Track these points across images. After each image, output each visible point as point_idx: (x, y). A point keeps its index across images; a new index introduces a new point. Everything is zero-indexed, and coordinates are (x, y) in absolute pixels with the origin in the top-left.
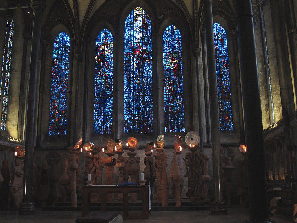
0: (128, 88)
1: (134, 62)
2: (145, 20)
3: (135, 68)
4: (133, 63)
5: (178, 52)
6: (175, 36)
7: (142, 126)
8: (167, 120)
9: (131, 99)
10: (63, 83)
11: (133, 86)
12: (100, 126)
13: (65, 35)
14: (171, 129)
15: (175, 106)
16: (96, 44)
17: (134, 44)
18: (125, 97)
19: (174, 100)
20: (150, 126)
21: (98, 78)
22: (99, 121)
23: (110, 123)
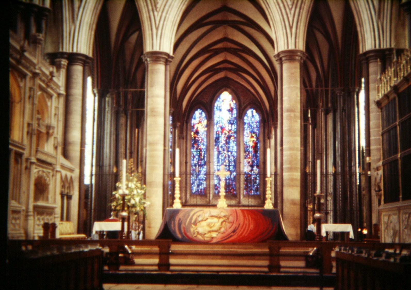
8: (247, 185)
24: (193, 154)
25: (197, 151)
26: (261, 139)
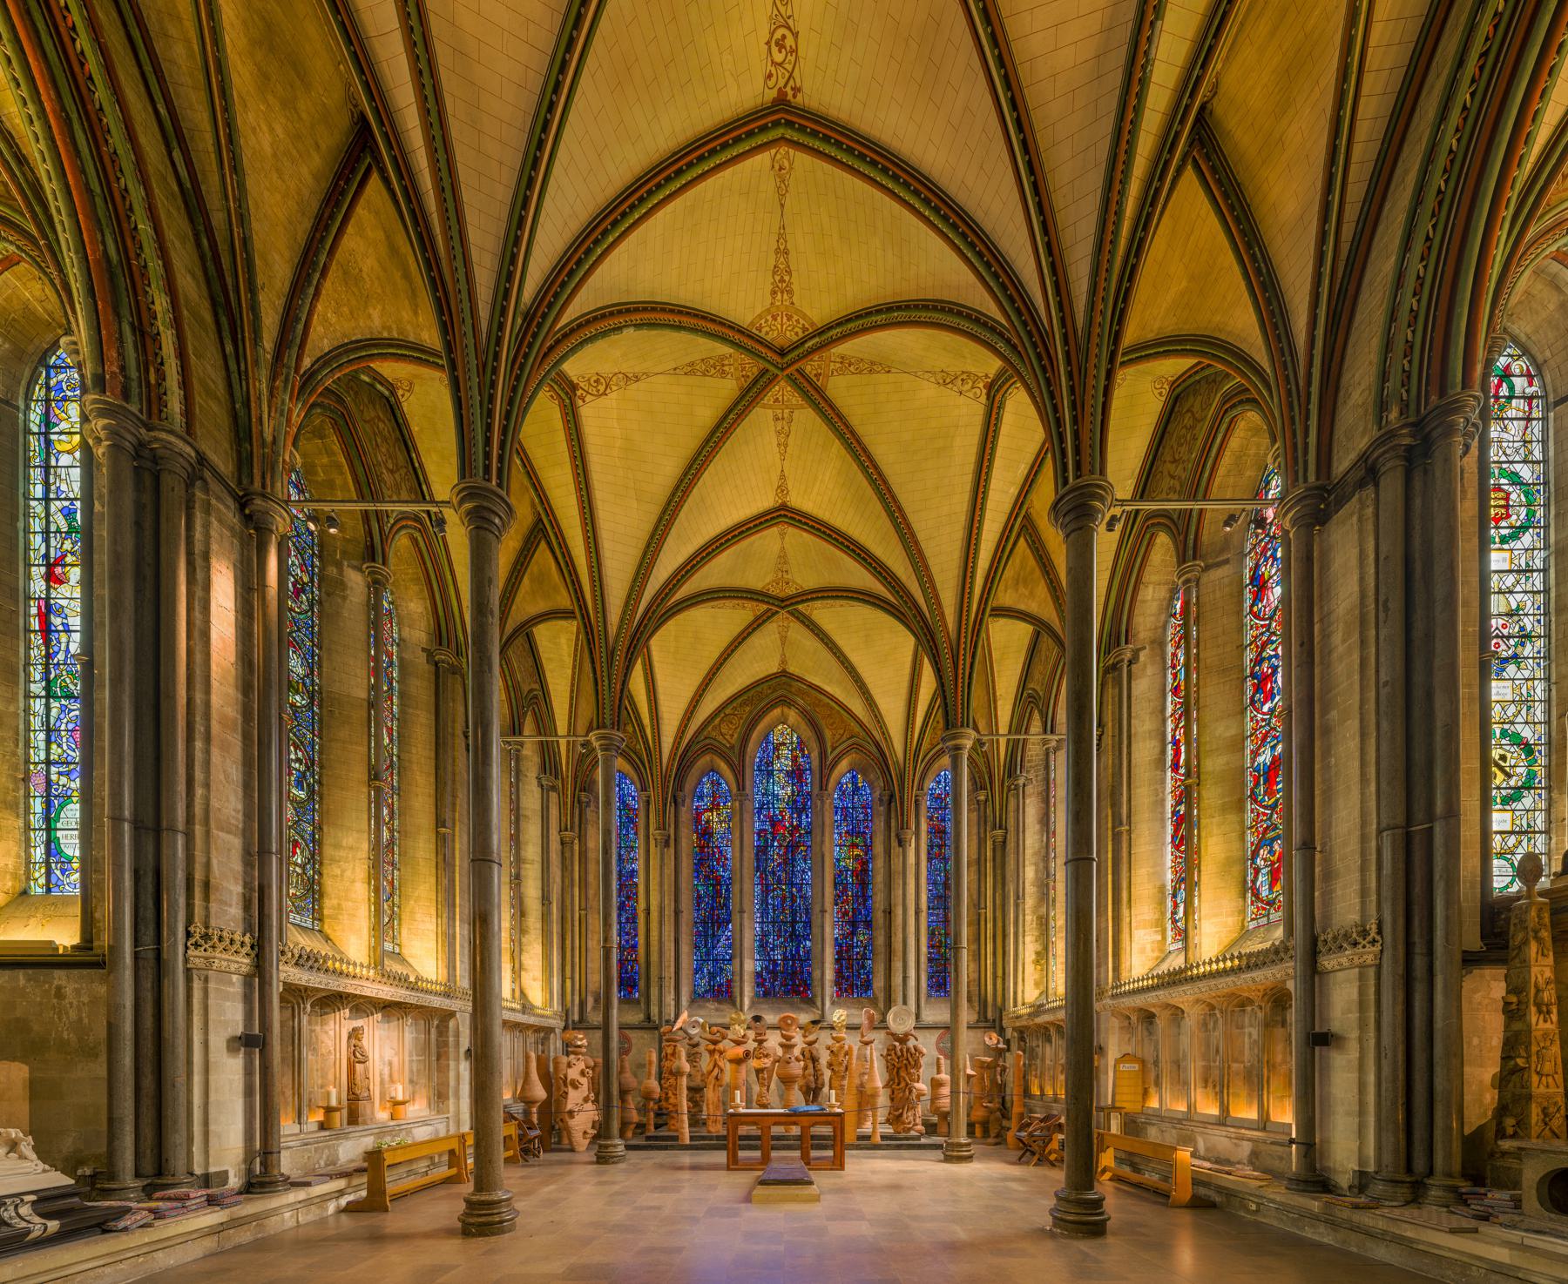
14: (846, 991)
19: (853, 933)
25: (707, 886)
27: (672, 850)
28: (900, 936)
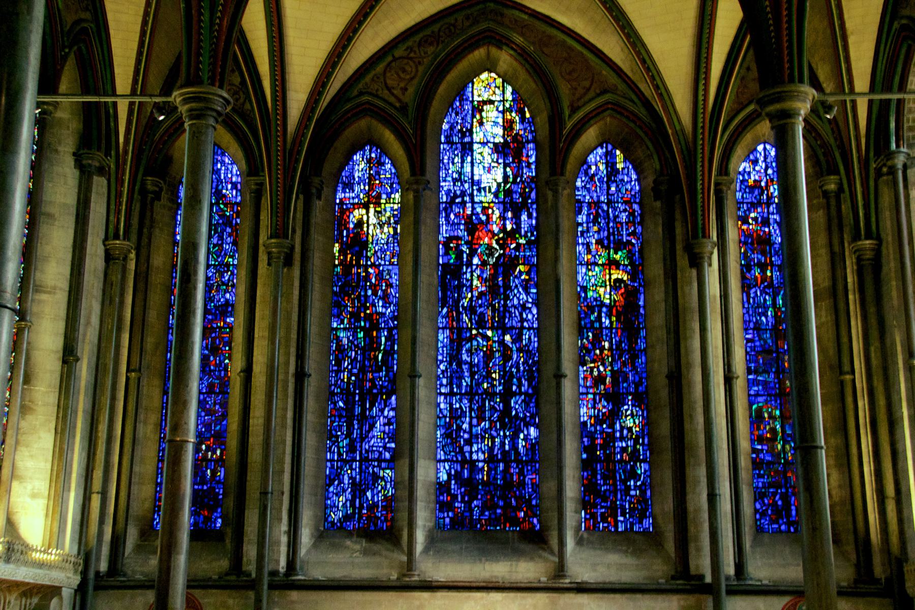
0: (450, 364)
1: (472, 272)
2: (512, 122)
3: (476, 294)
4: (468, 276)
5: (629, 242)
6: (617, 186)
7: (501, 503)
9: (461, 407)
10: (213, 335)
11: (469, 359)
12: (347, 500)
13: (219, 158)
14: (604, 520)
15: (618, 434)
16: (338, 201)
17: (473, 209)
18: (441, 399)
19: (614, 415)
20: (530, 506)
21: (342, 322)
22: (346, 482)
23: (384, 488)
24: (338, 339)
25: (354, 330)
26: (655, 269)
27: (296, 272)
28: (700, 419)
